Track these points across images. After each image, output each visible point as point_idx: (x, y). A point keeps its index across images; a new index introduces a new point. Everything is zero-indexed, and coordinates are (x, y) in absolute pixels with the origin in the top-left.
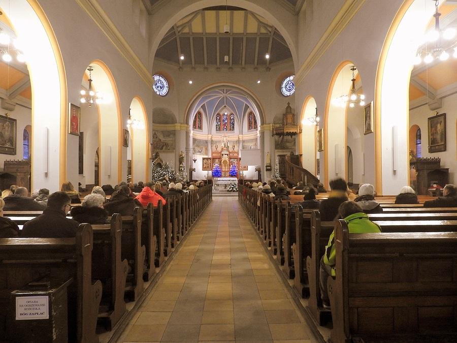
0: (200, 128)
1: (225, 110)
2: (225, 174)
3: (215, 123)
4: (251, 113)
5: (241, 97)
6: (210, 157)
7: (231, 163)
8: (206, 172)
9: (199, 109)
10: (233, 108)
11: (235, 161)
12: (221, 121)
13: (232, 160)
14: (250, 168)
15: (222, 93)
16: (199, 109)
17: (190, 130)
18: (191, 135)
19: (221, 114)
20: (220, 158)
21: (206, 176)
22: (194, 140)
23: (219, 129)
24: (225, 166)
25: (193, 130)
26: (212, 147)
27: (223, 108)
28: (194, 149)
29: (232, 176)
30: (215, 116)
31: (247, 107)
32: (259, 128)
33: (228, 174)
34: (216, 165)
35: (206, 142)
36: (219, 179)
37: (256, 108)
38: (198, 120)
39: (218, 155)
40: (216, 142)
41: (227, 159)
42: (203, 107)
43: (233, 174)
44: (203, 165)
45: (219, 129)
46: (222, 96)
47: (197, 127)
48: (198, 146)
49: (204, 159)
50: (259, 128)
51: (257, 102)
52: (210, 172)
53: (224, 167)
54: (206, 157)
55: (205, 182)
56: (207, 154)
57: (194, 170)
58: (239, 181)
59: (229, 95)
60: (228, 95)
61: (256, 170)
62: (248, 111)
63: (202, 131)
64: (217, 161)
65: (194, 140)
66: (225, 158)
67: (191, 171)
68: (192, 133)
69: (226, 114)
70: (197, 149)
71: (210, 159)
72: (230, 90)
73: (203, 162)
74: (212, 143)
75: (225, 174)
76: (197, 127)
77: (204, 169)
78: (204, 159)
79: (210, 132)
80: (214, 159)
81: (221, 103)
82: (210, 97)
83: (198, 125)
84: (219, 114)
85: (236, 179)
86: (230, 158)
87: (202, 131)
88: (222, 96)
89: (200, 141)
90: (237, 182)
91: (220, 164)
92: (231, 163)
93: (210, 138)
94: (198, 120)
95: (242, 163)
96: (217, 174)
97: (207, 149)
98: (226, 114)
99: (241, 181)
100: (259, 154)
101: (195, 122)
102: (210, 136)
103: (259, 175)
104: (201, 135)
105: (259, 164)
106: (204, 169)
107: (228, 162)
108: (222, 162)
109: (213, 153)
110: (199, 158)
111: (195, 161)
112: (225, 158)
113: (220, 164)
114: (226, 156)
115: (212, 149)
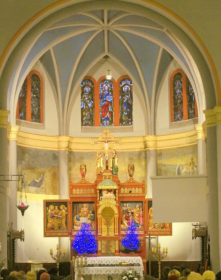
0: (38, 117)
1: (106, 66)
2: (108, 247)
3: (77, 106)
4: (179, 77)
5: (145, 31)
6: (65, 196)
7: (124, 215)
8: (53, 242)
9: (35, 65)
10: (127, 61)
11: (136, 210)
12: (97, 97)
13: (127, 207)
14: (177, 227)
15: (101, 22)
16: (35, 65)
17: (9, 123)
18: (13, 136)
19: (96, 77)
20: (93, 202)
21: (55, 252)
22: (22, 151)
23: (88, 120)
24: (108, 224)
25: (18, 123)
26: (70, 169)
27: (100, 64)
28: (20, 175)
29: (126, 252)
30: (79, 84)
31: (167, 59)
32: (202, 117)
33: (115, 246)
34: (83, 220)
35: (55, 156)
36: (91, 260)
37: (202, 90)
38: (30, 94)
39: (88, 193)
40: (82, 156)
41: (113, 204)
42: (46, 60)
43: (131, 245)
44: (46, 221)
45: (88, 120)
46: (97, 27)
47: (29, 115)
48: (31, 168)
49: (47, 204)
50: (202, 117)
51: (206, 65)
52: (66, 242)
53: (104, 227)
54: (55, 197)
55: (50, 268)
56: (55, 190)
57: (21, 235)
58: (147, 265)
59: (116, 27)
60: (114, 27)
61: (196, 234)
62: (171, 69)
63: (44, 128)
64: (85, 208)
65: (22, 151)
66: (108, 201)
67: (14, 237)
68: (15, 132)
69: (109, 77)
70: (29, 176)
71: (65, 203)
72: (120, 13)
73: (46, 212)
74: (70, 160)
75: (108, 247)
76: (29, 115)
77: (49, 231)
78: (47, 204)
79: (64, 129)
80: (76, 203)
81: (96, 47)
82: (64, 31)
83: (31, 109)
84: (88, 80)
85: (138, 259)
86: (121, 201)
87: (44, 128)
88: (97, 27)
89: (37, 154)
90: (141, 270)
91: (95, 219)
92: (124, 215)
93: (64, 145)
94: (30, 94)
95: (156, 217)
96: (85, 244)
97: (56, 177)
98: (109, 77)
99: (152, 267)
100: (203, 188)
101: (22, 100)
102: (65, 139)
103: (205, 249)
104: (40, 138)
105: (204, 218)
106: (49, 231)
107: (116, 211)
108: (100, 211)
109: (72, 187)
110: (35, 202)
111: (23, 209)
112: (108, 201)
113: (95, 219)
114: (111, 195)
115: (70, 175)
